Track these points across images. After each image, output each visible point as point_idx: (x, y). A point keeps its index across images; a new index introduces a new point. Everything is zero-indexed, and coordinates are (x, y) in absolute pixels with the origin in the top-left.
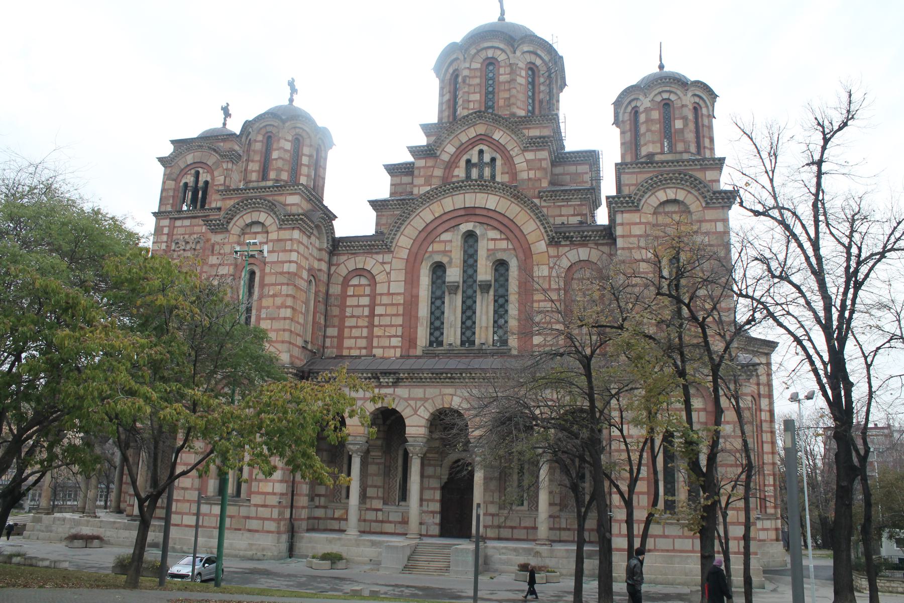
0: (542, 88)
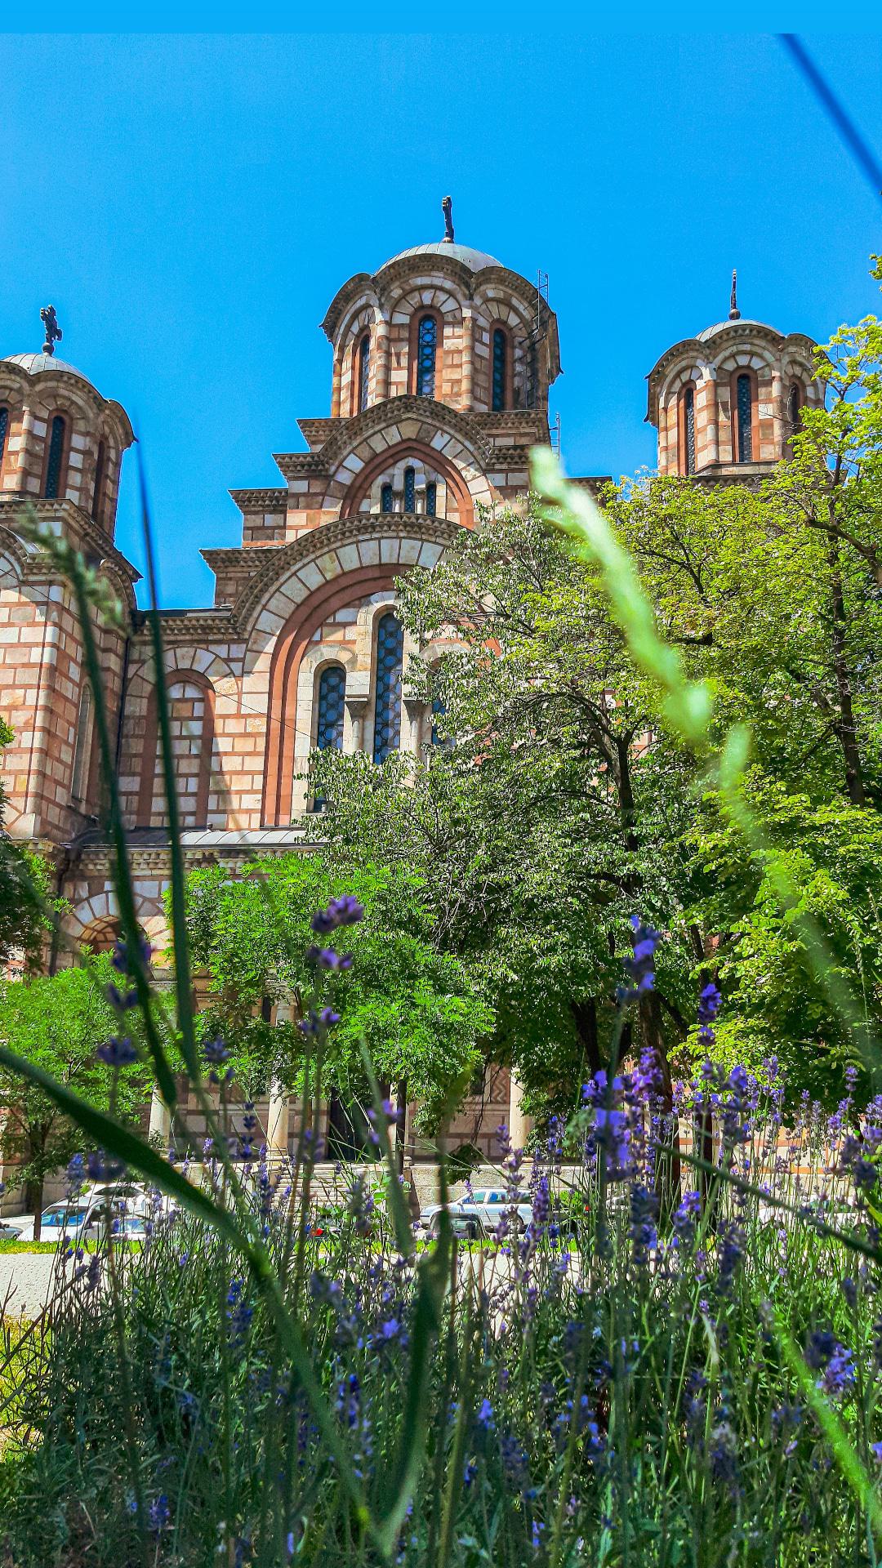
0: (519, 368)
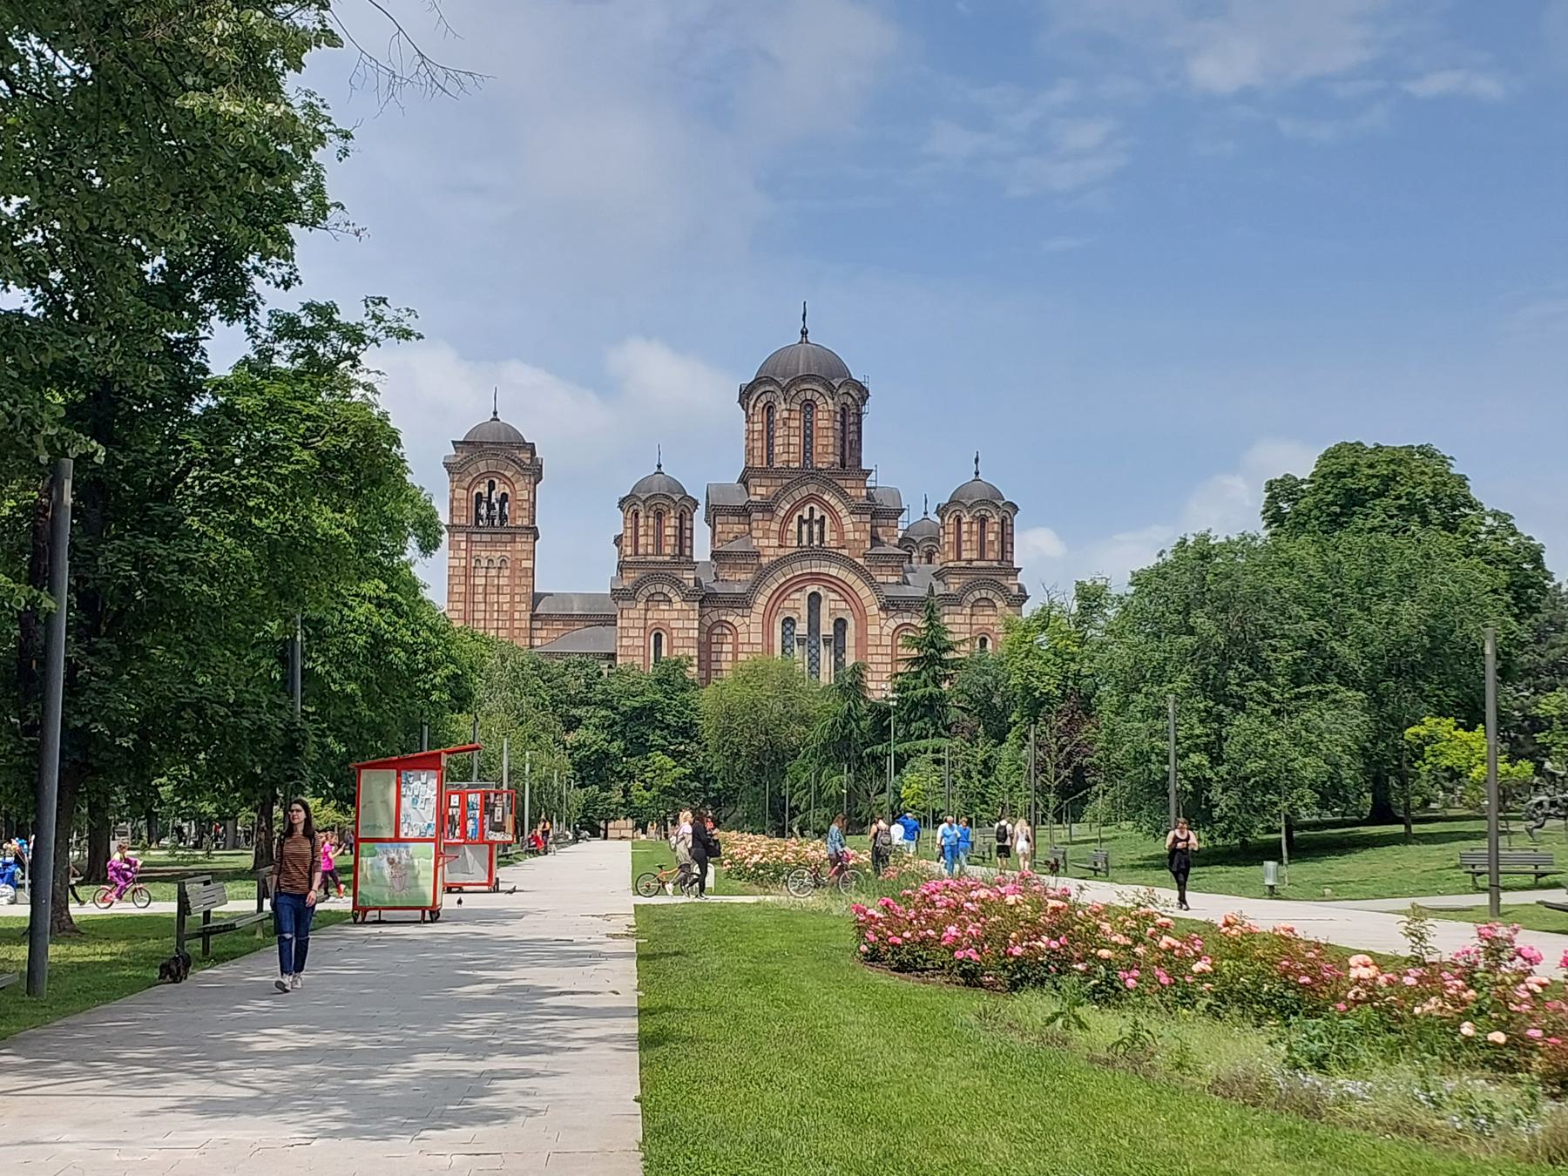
0: (853, 428)
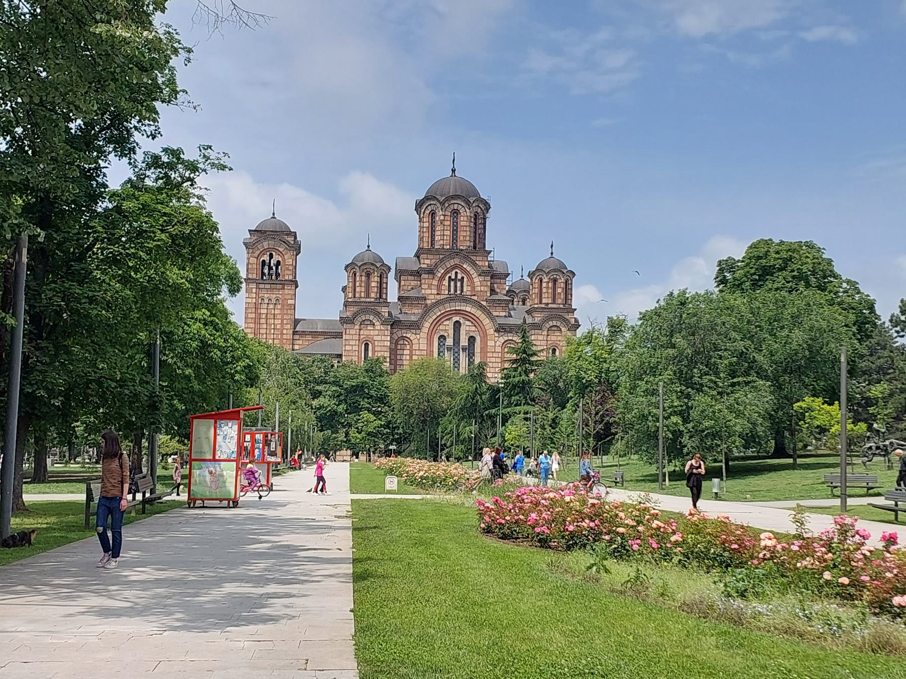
0: (481, 226)
